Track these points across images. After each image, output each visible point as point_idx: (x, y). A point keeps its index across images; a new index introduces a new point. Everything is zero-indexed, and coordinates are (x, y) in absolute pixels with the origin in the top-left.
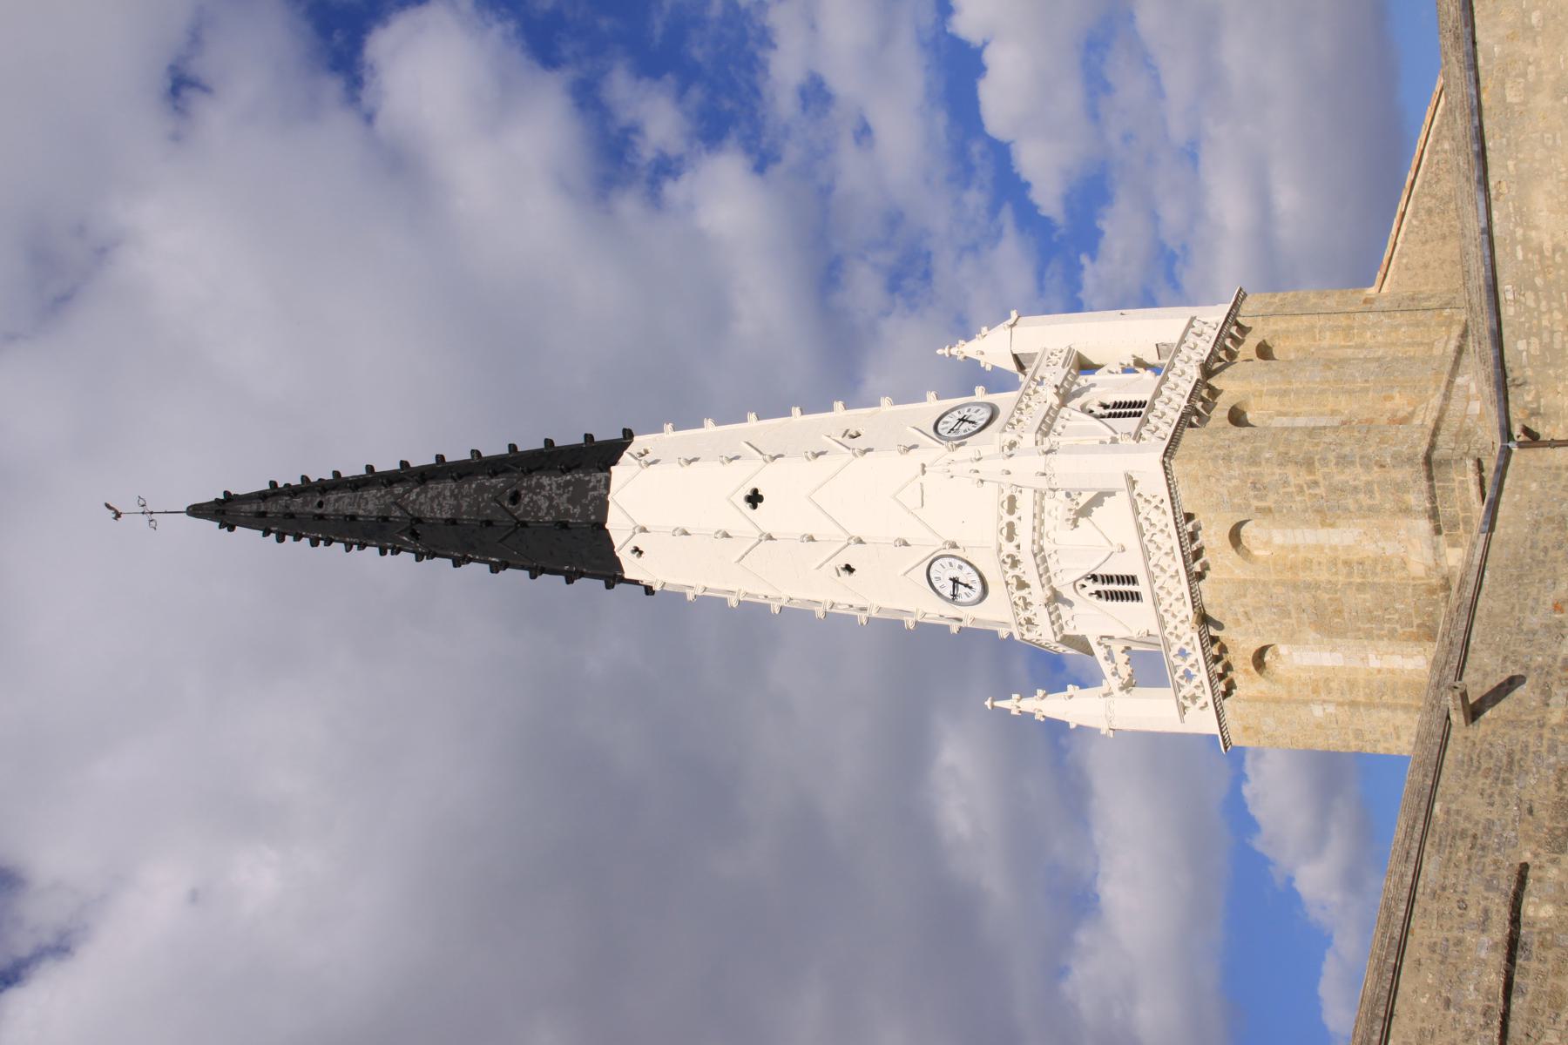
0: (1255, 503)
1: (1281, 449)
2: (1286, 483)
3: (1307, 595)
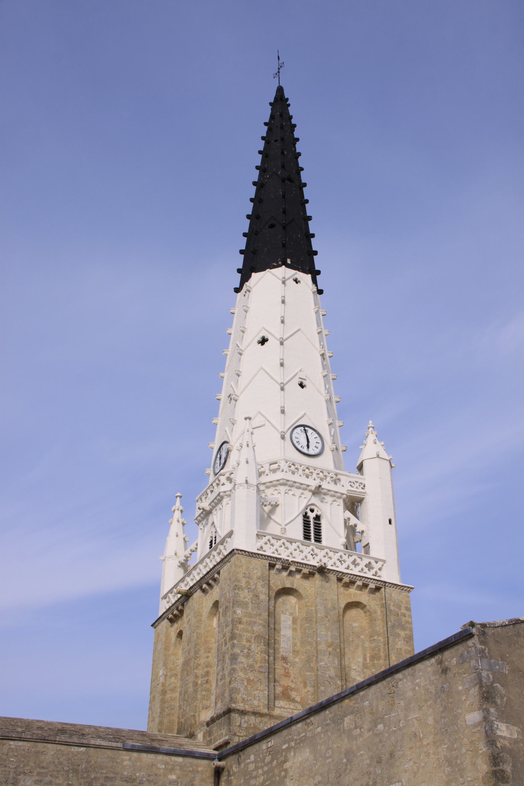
1: (244, 620)
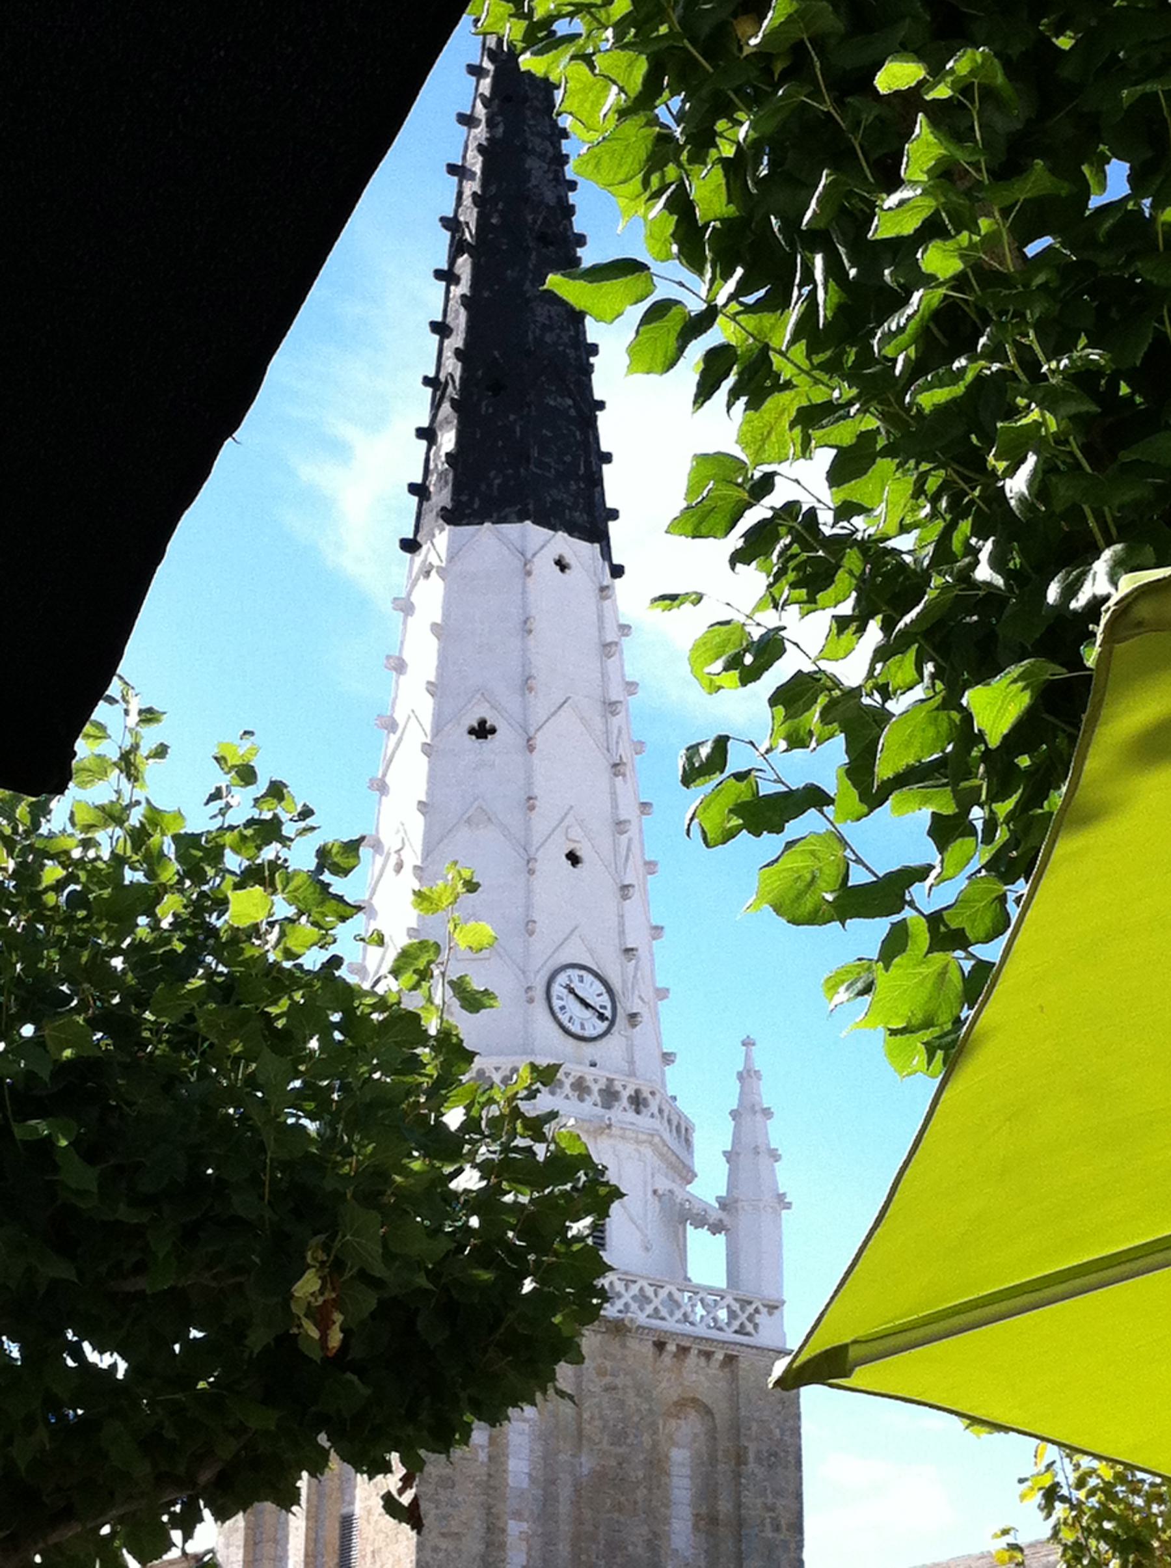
0: (752, 1448)
2: (778, 1494)
3: (641, 1474)
